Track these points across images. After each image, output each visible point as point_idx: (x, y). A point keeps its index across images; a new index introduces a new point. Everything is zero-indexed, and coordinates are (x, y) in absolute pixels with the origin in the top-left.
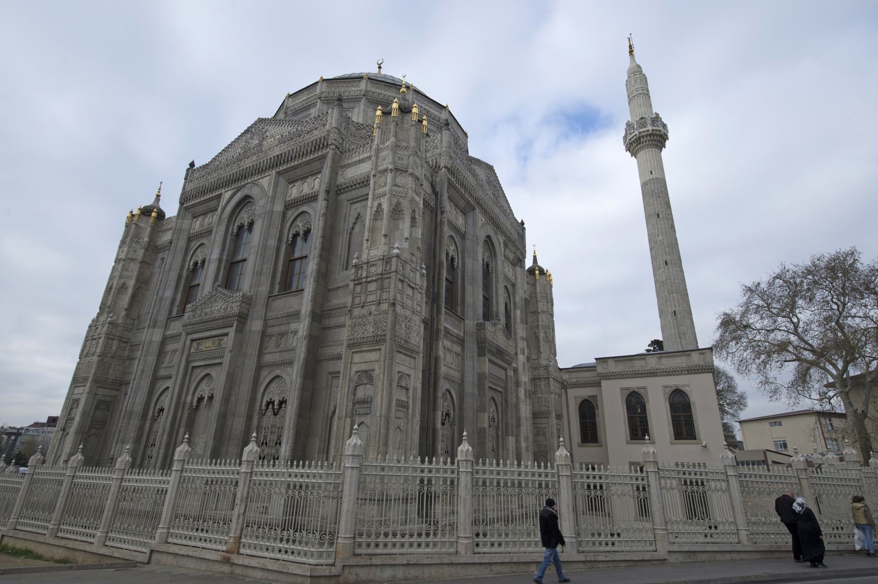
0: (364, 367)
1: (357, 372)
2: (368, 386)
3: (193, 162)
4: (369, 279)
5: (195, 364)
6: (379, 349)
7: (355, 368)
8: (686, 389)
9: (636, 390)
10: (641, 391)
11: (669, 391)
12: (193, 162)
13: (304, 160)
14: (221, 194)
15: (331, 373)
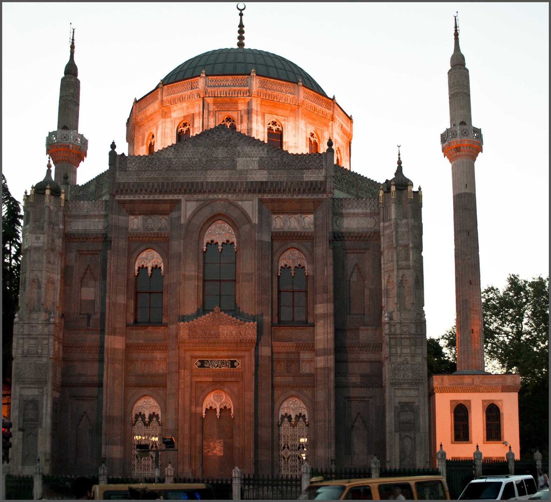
0: (405, 400)
1: (399, 403)
2: (409, 413)
3: (113, 143)
4: (403, 336)
5: (198, 379)
6: (418, 389)
7: (397, 401)
8: (499, 404)
9: (462, 403)
10: (466, 404)
11: (487, 404)
12: (113, 143)
13: (295, 197)
14: (179, 201)
15: (346, 397)
